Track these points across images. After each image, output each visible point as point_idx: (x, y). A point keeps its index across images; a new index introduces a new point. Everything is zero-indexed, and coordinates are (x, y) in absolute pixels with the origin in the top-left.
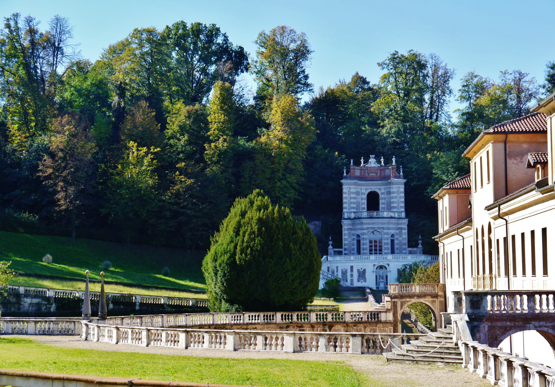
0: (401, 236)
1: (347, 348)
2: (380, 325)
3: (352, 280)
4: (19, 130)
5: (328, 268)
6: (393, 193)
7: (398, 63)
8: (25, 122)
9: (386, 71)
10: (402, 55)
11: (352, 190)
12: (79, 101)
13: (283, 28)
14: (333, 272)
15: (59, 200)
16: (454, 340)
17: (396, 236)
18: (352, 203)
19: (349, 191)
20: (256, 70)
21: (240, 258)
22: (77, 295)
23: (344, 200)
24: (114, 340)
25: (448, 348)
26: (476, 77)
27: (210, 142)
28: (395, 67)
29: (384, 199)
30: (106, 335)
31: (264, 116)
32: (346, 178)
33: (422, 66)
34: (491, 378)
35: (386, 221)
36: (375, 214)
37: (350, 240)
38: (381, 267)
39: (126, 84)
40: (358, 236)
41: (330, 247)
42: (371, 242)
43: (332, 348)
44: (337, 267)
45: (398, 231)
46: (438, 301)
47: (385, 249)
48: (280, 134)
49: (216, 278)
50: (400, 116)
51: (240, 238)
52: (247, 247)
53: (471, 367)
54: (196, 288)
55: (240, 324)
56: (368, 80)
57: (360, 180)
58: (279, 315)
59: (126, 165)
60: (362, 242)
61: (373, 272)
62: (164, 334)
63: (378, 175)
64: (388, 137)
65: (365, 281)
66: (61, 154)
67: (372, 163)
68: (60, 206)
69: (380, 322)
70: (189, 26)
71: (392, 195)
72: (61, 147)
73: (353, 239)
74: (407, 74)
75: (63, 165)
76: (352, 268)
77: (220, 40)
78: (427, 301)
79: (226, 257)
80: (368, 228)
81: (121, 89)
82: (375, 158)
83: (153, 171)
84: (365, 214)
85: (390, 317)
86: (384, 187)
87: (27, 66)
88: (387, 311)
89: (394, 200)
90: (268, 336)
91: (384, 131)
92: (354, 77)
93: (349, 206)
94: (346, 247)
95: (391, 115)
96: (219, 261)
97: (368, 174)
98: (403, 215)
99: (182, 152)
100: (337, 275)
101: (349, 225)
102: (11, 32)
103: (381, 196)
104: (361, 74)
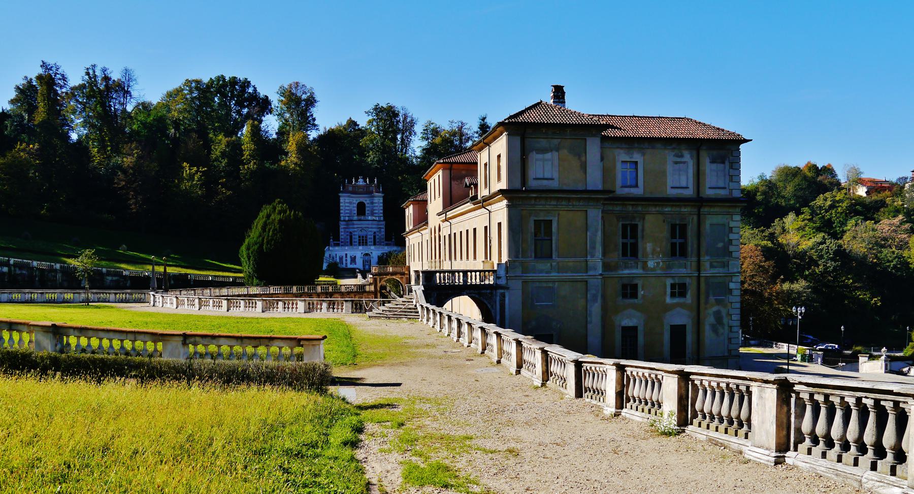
0: (380, 233)
1: (342, 309)
2: (365, 294)
3: (346, 264)
4: (98, 152)
5: (330, 255)
6: (375, 203)
7: (379, 112)
8: (102, 148)
9: (370, 118)
10: (382, 107)
11: (346, 201)
12: (144, 132)
13: (297, 83)
14: (333, 258)
15: (131, 205)
16: (414, 303)
17: (377, 233)
18: (346, 210)
20: (277, 113)
21: (266, 248)
22: (146, 274)
23: (341, 208)
24: (175, 306)
25: (410, 309)
26: (432, 124)
27: (244, 164)
28: (377, 115)
29: (369, 207)
30: (169, 302)
31: (284, 146)
32: (342, 192)
33: (396, 115)
34: (437, 327)
35: (370, 222)
36: (362, 217)
37: (345, 235)
38: (367, 255)
39: (180, 120)
40: (351, 233)
41: (331, 240)
42: (359, 237)
43: (331, 310)
44: (336, 254)
45: (378, 230)
46: (405, 277)
47: (370, 242)
48: (295, 160)
49: (250, 262)
50: (380, 149)
51: (266, 234)
52: (272, 240)
53: (425, 320)
54: (235, 269)
55: (267, 294)
56: (358, 123)
57: (353, 194)
58: (295, 288)
59: (182, 179)
60: (353, 237)
61: (361, 258)
62: (211, 301)
64: (371, 164)
65: (356, 264)
66: (131, 171)
67: (361, 182)
68: (132, 209)
69: (365, 292)
70: (227, 79)
71: (375, 205)
72: (131, 165)
73: (347, 235)
74: (385, 120)
75: (133, 179)
76: (346, 255)
77: (251, 90)
78: (397, 278)
79: (256, 247)
80: (358, 227)
81: (176, 124)
82: (363, 178)
83: (202, 185)
84: (355, 218)
85: (372, 288)
86: (369, 199)
87: (103, 105)
88: (370, 284)
89: (376, 208)
90: (287, 302)
91: (369, 160)
92: (348, 121)
95: (374, 149)
96: (251, 250)
98: (382, 218)
99: (223, 171)
100: (336, 260)
101: (345, 225)
102: (90, 78)
103: (366, 205)
104: (353, 119)
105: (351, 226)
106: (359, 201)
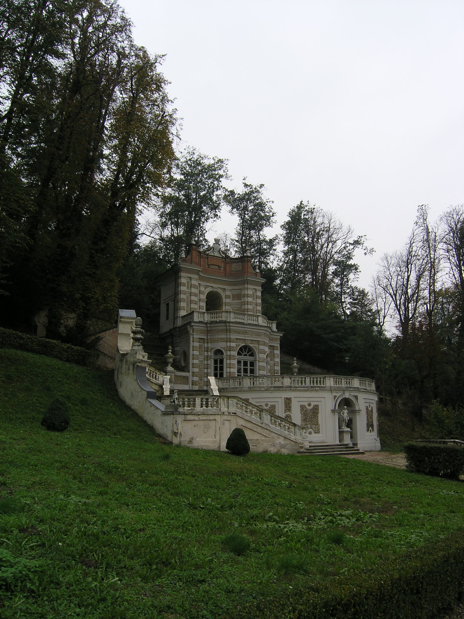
6: (248, 296)
11: (194, 282)
19: (188, 283)
29: (230, 304)
37: (201, 358)
40: (218, 352)
42: (239, 362)
61: (333, 411)
63: (222, 269)
71: (243, 300)
73: (207, 358)
76: (288, 402)
93: (187, 305)
94: (196, 370)
97: (208, 265)
101: (201, 332)
103: (225, 300)
105: (224, 336)
106: (212, 290)
